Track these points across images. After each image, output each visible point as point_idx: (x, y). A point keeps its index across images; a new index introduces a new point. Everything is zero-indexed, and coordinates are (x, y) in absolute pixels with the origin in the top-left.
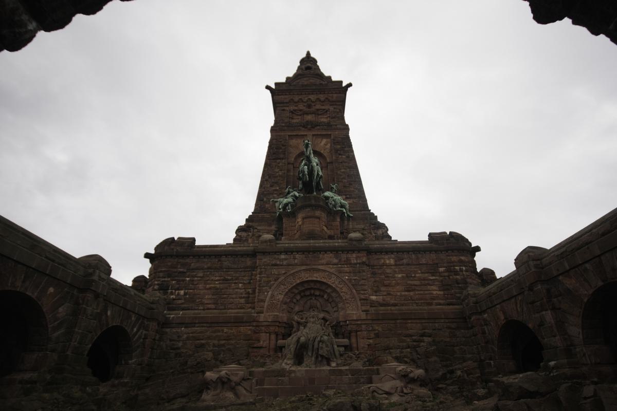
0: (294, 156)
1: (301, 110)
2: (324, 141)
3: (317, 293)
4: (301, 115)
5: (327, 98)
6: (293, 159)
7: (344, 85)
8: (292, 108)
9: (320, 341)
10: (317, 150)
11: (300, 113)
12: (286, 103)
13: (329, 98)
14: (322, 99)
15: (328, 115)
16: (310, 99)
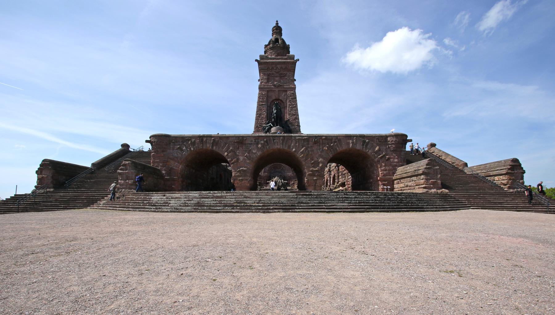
0: (270, 102)
1: (273, 74)
2: (284, 93)
3: (279, 167)
4: (273, 77)
5: (286, 67)
6: (269, 104)
7: (295, 59)
8: (269, 72)
9: (279, 182)
10: (281, 99)
11: (273, 76)
12: (266, 69)
13: (287, 67)
14: (284, 67)
15: (286, 77)
16: (277, 67)
